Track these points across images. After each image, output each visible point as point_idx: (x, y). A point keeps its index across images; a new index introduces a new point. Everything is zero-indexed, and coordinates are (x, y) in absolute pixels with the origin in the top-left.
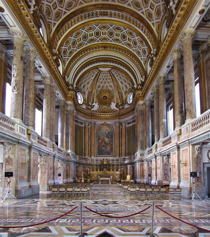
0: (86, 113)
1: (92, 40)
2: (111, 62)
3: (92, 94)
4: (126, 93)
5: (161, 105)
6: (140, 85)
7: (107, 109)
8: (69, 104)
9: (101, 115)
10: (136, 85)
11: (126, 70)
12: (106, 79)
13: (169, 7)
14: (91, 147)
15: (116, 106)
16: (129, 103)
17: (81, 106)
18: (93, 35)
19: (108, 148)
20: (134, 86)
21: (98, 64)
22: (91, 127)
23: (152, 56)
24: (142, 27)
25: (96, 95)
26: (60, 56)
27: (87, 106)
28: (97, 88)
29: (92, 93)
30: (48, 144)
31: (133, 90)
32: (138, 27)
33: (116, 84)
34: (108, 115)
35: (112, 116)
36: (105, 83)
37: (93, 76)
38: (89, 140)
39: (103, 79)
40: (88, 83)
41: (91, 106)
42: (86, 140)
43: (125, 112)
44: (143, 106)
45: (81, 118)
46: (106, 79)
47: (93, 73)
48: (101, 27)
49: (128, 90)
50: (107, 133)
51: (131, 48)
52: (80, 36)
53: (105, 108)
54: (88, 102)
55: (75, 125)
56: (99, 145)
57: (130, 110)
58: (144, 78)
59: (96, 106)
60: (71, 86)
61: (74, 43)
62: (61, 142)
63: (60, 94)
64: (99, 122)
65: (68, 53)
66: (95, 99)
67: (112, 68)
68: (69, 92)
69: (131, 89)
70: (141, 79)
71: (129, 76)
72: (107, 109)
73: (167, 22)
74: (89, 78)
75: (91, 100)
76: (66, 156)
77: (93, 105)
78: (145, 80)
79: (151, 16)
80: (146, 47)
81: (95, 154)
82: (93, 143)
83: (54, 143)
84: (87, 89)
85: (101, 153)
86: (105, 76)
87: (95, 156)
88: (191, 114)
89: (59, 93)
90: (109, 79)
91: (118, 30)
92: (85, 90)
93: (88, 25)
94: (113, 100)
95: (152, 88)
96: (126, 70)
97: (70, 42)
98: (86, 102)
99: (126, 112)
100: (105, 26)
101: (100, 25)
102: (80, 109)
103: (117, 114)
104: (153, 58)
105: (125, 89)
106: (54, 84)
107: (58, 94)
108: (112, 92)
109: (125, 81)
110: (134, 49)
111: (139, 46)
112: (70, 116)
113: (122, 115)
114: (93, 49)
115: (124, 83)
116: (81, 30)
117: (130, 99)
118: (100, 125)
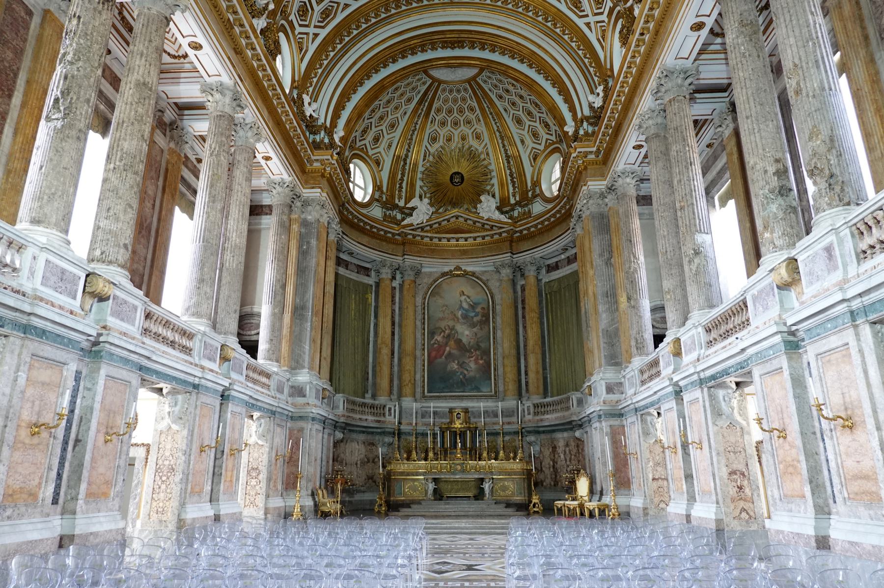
0: (382, 233)
2: (474, 48)
3: (407, 168)
4: (535, 159)
6: (587, 121)
8: (313, 200)
10: (573, 124)
11: (532, 73)
12: (461, 111)
14: (400, 360)
15: (498, 208)
17: (364, 211)
19: (472, 365)
20: (566, 129)
22: (401, 286)
23: (629, 4)
26: (283, 22)
27: (387, 209)
28: (425, 143)
29: (408, 161)
31: (561, 144)
33: (496, 128)
34: (470, 241)
36: (456, 124)
37: (409, 100)
38: (393, 334)
39: (450, 111)
40: (392, 126)
41: (401, 210)
42: (380, 335)
43: (532, 229)
44: (607, 200)
46: (461, 111)
47: (411, 87)
49: (542, 147)
50: (465, 305)
53: (457, 217)
55: (337, 274)
56: (434, 354)
57: (552, 219)
58: (602, 94)
59: (423, 211)
60: (323, 133)
62: (272, 340)
63: (275, 159)
64: (432, 267)
65: (316, 16)
66: (419, 183)
67: (482, 70)
68: (316, 152)
69: (554, 143)
70: (591, 98)
72: (466, 220)
74: (396, 108)
75: (404, 190)
76: (291, 395)
78: (606, 99)
81: (419, 390)
82: (409, 345)
83: (233, 342)
84: (390, 146)
85: (440, 381)
86: (455, 101)
87: (418, 395)
88: (838, 189)
89: (272, 154)
90: (472, 109)
94: (488, 188)
95: (636, 121)
96: (532, 73)
98: (384, 196)
99: (540, 226)
102: (360, 220)
103: (504, 235)
104: (631, 9)
105: (532, 145)
106: (250, 114)
107: (268, 158)
108: (482, 157)
109: (530, 113)
112: (314, 242)
113: (523, 238)
115: (528, 123)
117: (553, 180)
118: (437, 275)
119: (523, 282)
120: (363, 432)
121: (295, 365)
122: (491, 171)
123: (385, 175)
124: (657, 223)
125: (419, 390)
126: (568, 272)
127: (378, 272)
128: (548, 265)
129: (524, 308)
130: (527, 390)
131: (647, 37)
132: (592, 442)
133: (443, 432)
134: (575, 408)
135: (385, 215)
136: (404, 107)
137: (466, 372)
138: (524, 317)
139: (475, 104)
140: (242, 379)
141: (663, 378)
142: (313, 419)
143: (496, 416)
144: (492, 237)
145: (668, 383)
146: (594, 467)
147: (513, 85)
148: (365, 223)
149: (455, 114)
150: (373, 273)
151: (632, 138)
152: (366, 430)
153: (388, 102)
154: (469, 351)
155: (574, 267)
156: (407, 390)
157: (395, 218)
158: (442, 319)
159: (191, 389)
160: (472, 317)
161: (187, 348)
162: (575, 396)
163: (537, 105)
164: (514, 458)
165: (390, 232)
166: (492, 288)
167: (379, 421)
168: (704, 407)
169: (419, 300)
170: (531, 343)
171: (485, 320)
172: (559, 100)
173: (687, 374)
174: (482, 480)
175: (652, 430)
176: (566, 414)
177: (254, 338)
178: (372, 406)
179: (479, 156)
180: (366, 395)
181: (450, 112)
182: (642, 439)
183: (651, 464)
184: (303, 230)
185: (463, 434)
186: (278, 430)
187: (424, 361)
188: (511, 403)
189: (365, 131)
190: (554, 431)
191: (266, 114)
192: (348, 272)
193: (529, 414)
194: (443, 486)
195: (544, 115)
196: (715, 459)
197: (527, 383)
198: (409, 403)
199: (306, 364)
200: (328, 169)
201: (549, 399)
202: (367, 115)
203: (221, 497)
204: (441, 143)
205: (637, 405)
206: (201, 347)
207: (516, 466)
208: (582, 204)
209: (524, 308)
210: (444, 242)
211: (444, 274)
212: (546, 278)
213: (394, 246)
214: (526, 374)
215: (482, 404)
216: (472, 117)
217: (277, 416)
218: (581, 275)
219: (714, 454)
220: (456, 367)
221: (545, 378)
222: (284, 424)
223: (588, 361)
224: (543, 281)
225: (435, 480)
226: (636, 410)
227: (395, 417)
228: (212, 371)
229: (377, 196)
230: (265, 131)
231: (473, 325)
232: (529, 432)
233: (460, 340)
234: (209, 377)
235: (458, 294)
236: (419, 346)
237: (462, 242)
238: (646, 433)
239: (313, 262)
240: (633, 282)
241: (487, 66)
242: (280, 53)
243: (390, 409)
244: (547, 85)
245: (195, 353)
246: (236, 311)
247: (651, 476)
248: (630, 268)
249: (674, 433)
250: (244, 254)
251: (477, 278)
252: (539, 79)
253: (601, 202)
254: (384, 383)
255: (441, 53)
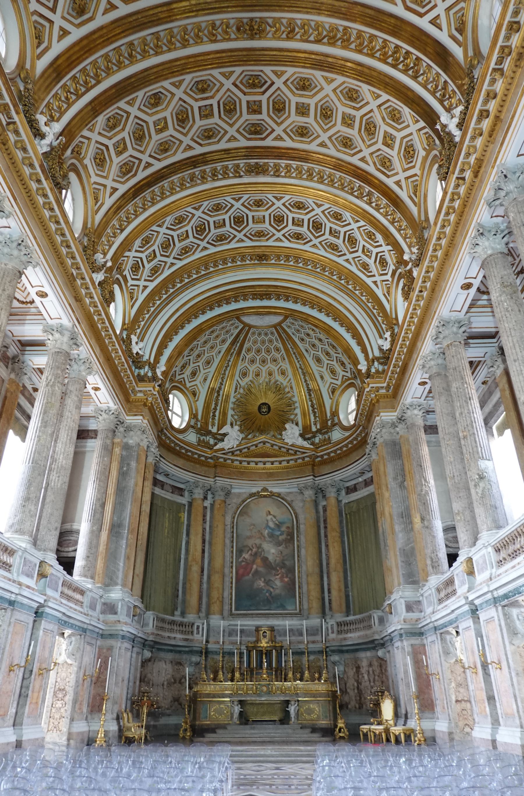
0: (196, 456)
1: (221, 238)
3: (220, 398)
4: (333, 392)
5: (461, 413)
6: (378, 361)
7: (272, 445)
9: (249, 463)
10: (366, 363)
11: (329, 321)
12: (268, 351)
13: (438, 127)
14: (209, 577)
15: (301, 435)
16: (345, 423)
17: (180, 436)
18: (224, 225)
19: (278, 583)
20: (359, 367)
21: (242, 304)
22: (212, 505)
23: (408, 268)
24: (369, 194)
25: (232, 400)
26: (118, 276)
27: (202, 435)
28: (237, 377)
30: (15, 561)
31: (356, 380)
32: (357, 197)
33: (298, 366)
34: (276, 465)
35: (287, 468)
36: (264, 362)
37: (224, 341)
38: (203, 551)
39: (258, 351)
40: (208, 363)
41: (214, 436)
42: (191, 553)
43: (332, 455)
44: (398, 429)
45: (177, 472)
46: (268, 351)
47: (225, 330)
48: (248, 203)
49: (339, 382)
50: (271, 524)
51: (340, 256)
52: (184, 226)
53: (264, 443)
54: (207, 424)
55: (153, 494)
57: (350, 446)
58: (389, 339)
59: (233, 437)
60: (147, 368)
61: (166, 246)
62: (88, 557)
64: (241, 488)
66: (230, 412)
67: (286, 317)
68: (140, 384)
69: (349, 379)
70: (380, 342)
71: (338, 337)
72: (272, 445)
73: (440, 166)
74: (212, 348)
75: (217, 418)
76: (103, 612)
77: (222, 432)
79: (388, 164)
80: (386, 248)
81: (226, 607)
82: (218, 563)
83: (51, 559)
84: (205, 380)
85: (248, 599)
86: (263, 342)
87: (226, 613)
89: (101, 385)
90: (278, 350)
91: (299, 208)
92: (199, 385)
93: (212, 197)
94: (292, 417)
95: (419, 362)
96: (329, 321)
97: (155, 241)
98: (199, 424)
99: (339, 452)
100: (261, 200)
101: (246, 197)
102: (176, 444)
103: (307, 459)
104: (410, 271)
106: (85, 350)
107: (96, 389)
108: (287, 390)
109: (328, 354)
110: (349, 256)
111: (364, 246)
112: (133, 464)
113: (324, 462)
114: (225, 262)
115: (326, 362)
116: (189, 209)
117: (349, 411)
118: (245, 496)
119: (324, 503)
120: (171, 651)
121: (109, 582)
122: (294, 403)
123: (200, 405)
124: (443, 450)
125: (226, 607)
126: (366, 494)
127: (191, 492)
128: (348, 488)
129: (326, 527)
130: (331, 609)
131: (425, 294)
132: (395, 662)
133: (250, 651)
134: (376, 627)
135: (199, 440)
136: (219, 347)
137: (272, 590)
138: (326, 536)
139: (280, 345)
140: (57, 595)
141: (459, 597)
142: (123, 637)
143: (301, 634)
144: (296, 461)
145: (463, 602)
146: (398, 688)
147: (313, 330)
148: (181, 447)
149: (263, 354)
150: (186, 494)
151: (417, 375)
152: (175, 649)
153: (205, 342)
154: (275, 569)
155: (371, 489)
156: (215, 607)
157: (208, 443)
158: (250, 537)
159: (7, 605)
160: (278, 536)
161: (7, 564)
162: (376, 615)
163: (334, 347)
164: (319, 679)
165: (203, 456)
166: (296, 508)
167: (186, 640)
168: (500, 625)
169: (228, 519)
170: (333, 561)
171: (290, 538)
172: (353, 343)
173: (481, 592)
174: (287, 702)
175: (452, 649)
176: (368, 632)
177: (71, 555)
178: (181, 624)
179: (284, 389)
180: (176, 613)
181: (258, 351)
182: (443, 658)
183: (453, 685)
184: (124, 453)
185: (269, 654)
186: (88, 648)
187: (232, 578)
188: (315, 621)
189: (184, 367)
190: (357, 650)
191: (98, 351)
192: (163, 492)
193: (333, 632)
194: (250, 710)
195: (340, 356)
196: (515, 680)
197: (330, 600)
198: (216, 621)
199: (119, 581)
200: (150, 399)
201: (351, 618)
202: (186, 353)
203: (25, 720)
204: (250, 378)
205: (436, 624)
206: (20, 563)
207: (321, 687)
208: (376, 432)
209: (326, 527)
210: (253, 465)
211: (252, 495)
212: (346, 499)
213: (206, 469)
214: (329, 592)
215: (287, 623)
216: (278, 356)
217: (88, 633)
218: (377, 497)
219: (513, 674)
220: (262, 584)
221: (347, 596)
222: (93, 642)
223: (388, 580)
224: (343, 502)
225: (241, 702)
226: (435, 628)
227: (203, 635)
228: (28, 587)
229: (192, 423)
230: (96, 366)
231: (279, 544)
232: (333, 651)
233: (267, 558)
234: (25, 593)
235: (265, 515)
236: (228, 564)
237: (268, 465)
238: (447, 653)
239: (132, 483)
240: (425, 504)
241: (290, 314)
242: (114, 301)
243: (198, 627)
244: (342, 331)
245: (14, 569)
246: (56, 528)
247: (454, 698)
248: (422, 490)
249: (473, 652)
250: (68, 475)
251: (283, 499)
252: (335, 325)
253: (392, 431)
254: (193, 600)
255: (251, 303)
